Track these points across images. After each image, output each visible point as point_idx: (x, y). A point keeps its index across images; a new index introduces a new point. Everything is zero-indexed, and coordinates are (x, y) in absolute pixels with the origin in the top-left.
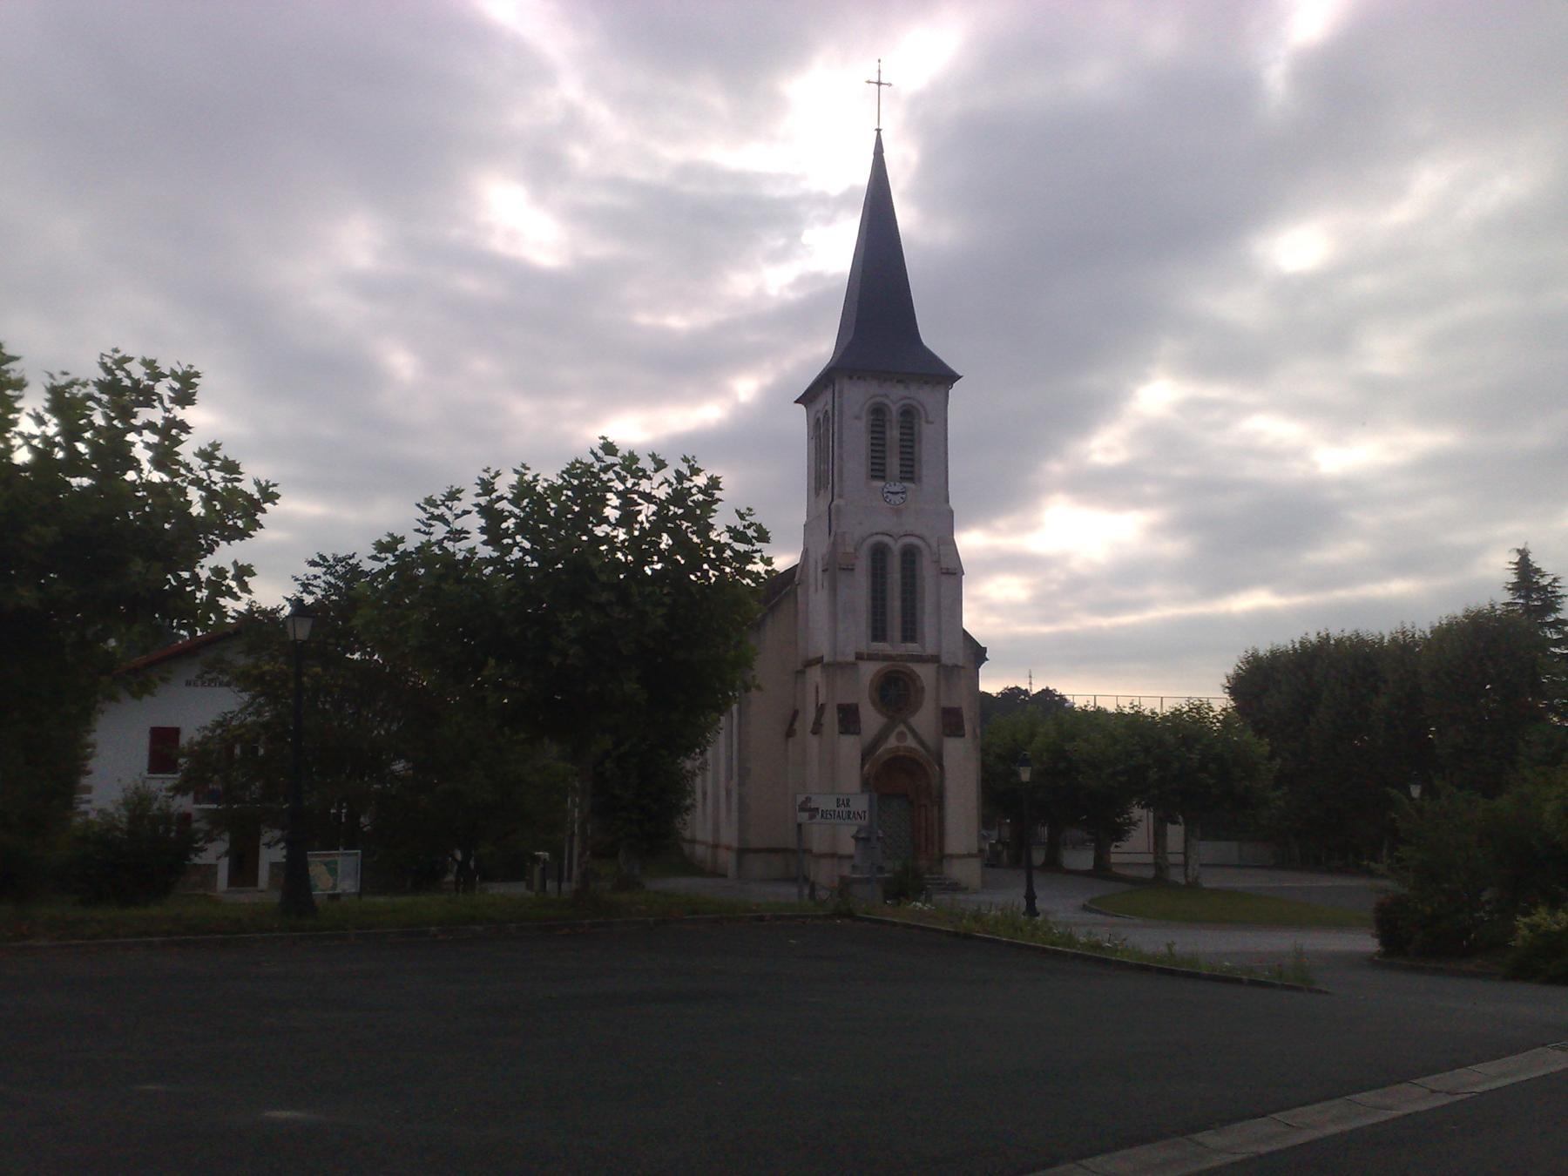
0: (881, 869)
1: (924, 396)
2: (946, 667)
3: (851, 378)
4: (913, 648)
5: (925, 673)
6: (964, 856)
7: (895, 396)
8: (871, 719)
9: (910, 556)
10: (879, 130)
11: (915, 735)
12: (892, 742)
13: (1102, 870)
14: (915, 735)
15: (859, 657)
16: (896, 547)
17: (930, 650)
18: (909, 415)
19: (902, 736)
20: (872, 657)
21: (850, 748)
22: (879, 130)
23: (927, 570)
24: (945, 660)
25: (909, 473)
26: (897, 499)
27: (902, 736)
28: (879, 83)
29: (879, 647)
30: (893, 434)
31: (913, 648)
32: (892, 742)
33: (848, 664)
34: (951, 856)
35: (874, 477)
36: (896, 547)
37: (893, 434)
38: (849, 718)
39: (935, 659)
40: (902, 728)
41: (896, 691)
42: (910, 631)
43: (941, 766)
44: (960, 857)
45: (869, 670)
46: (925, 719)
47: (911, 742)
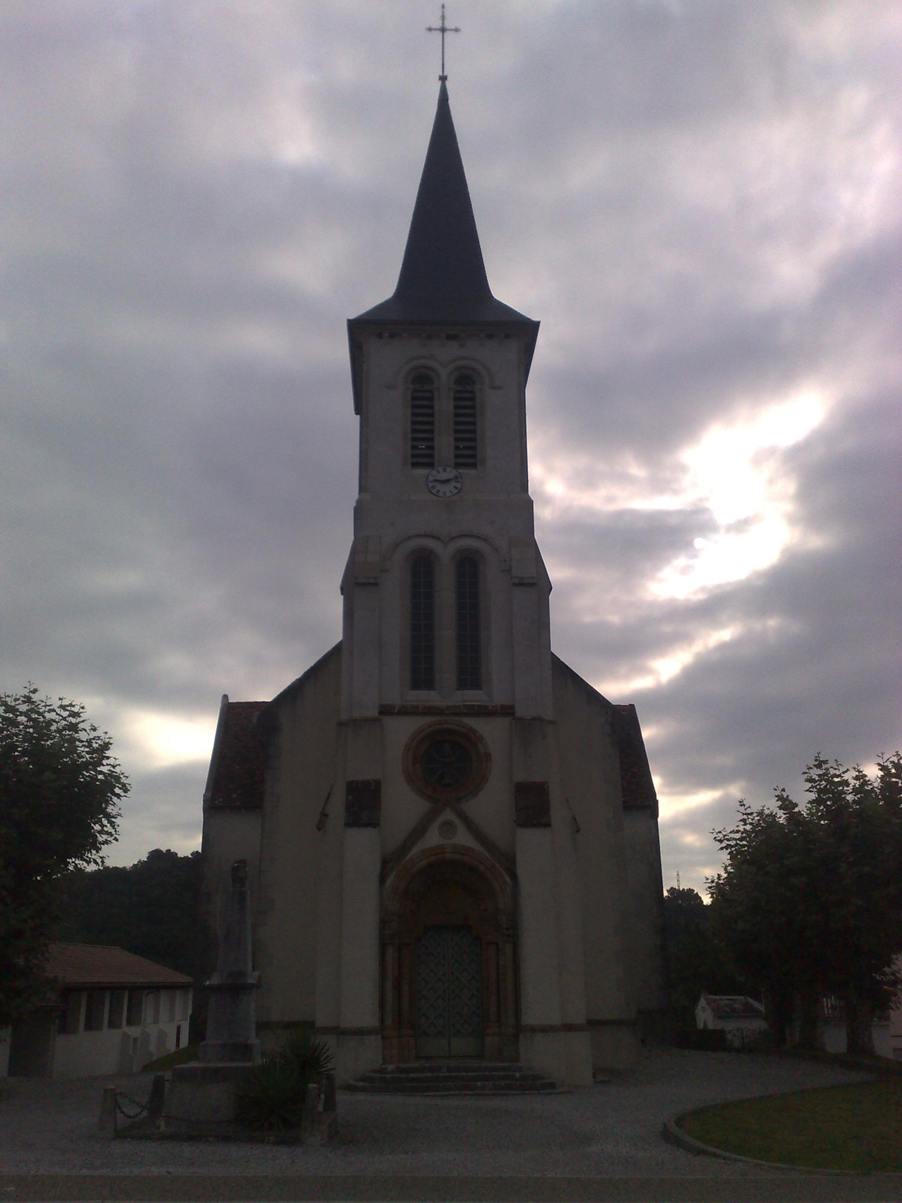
0: (245, 1050)
1: (489, 355)
2: (521, 719)
3: (380, 336)
4: (473, 697)
5: (492, 733)
6: (553, 1029)
7: (444, 357)
8: (403, 804)
9: (469, 566)
10: (443, 79)
11: (469, 824)
12: (433, 838)
13: (859, 1051)
14: (469, 824)
15: (386, 711)
16: (446, 554)
17: (499, 698)
18: (466, 382)
19: (448, 828)
20: (405, 711)
21: (362, 849)
22: (443, 79)
23: (493, 582)
24: (520, 711)
25: (468, 456)
26: (448, 490)
27: (448, 828)
28: (443, 30)
29: (424, 697)
30: (444, 406)
31: (473, 697)
32: (433, 838)
33: (373, 720)
34: (533, 1030)
35: (415, 465)
36: (446, 554)
37: (444, 406)
38: (363, 803)
39: (507, 711)
40: (448, 815)
41: (446, 762)
42: (471, 673)
43: (514, 876)
44: (546, 1030)
45: (402, 731)
46: (491, 804)
47: (463, 838)
